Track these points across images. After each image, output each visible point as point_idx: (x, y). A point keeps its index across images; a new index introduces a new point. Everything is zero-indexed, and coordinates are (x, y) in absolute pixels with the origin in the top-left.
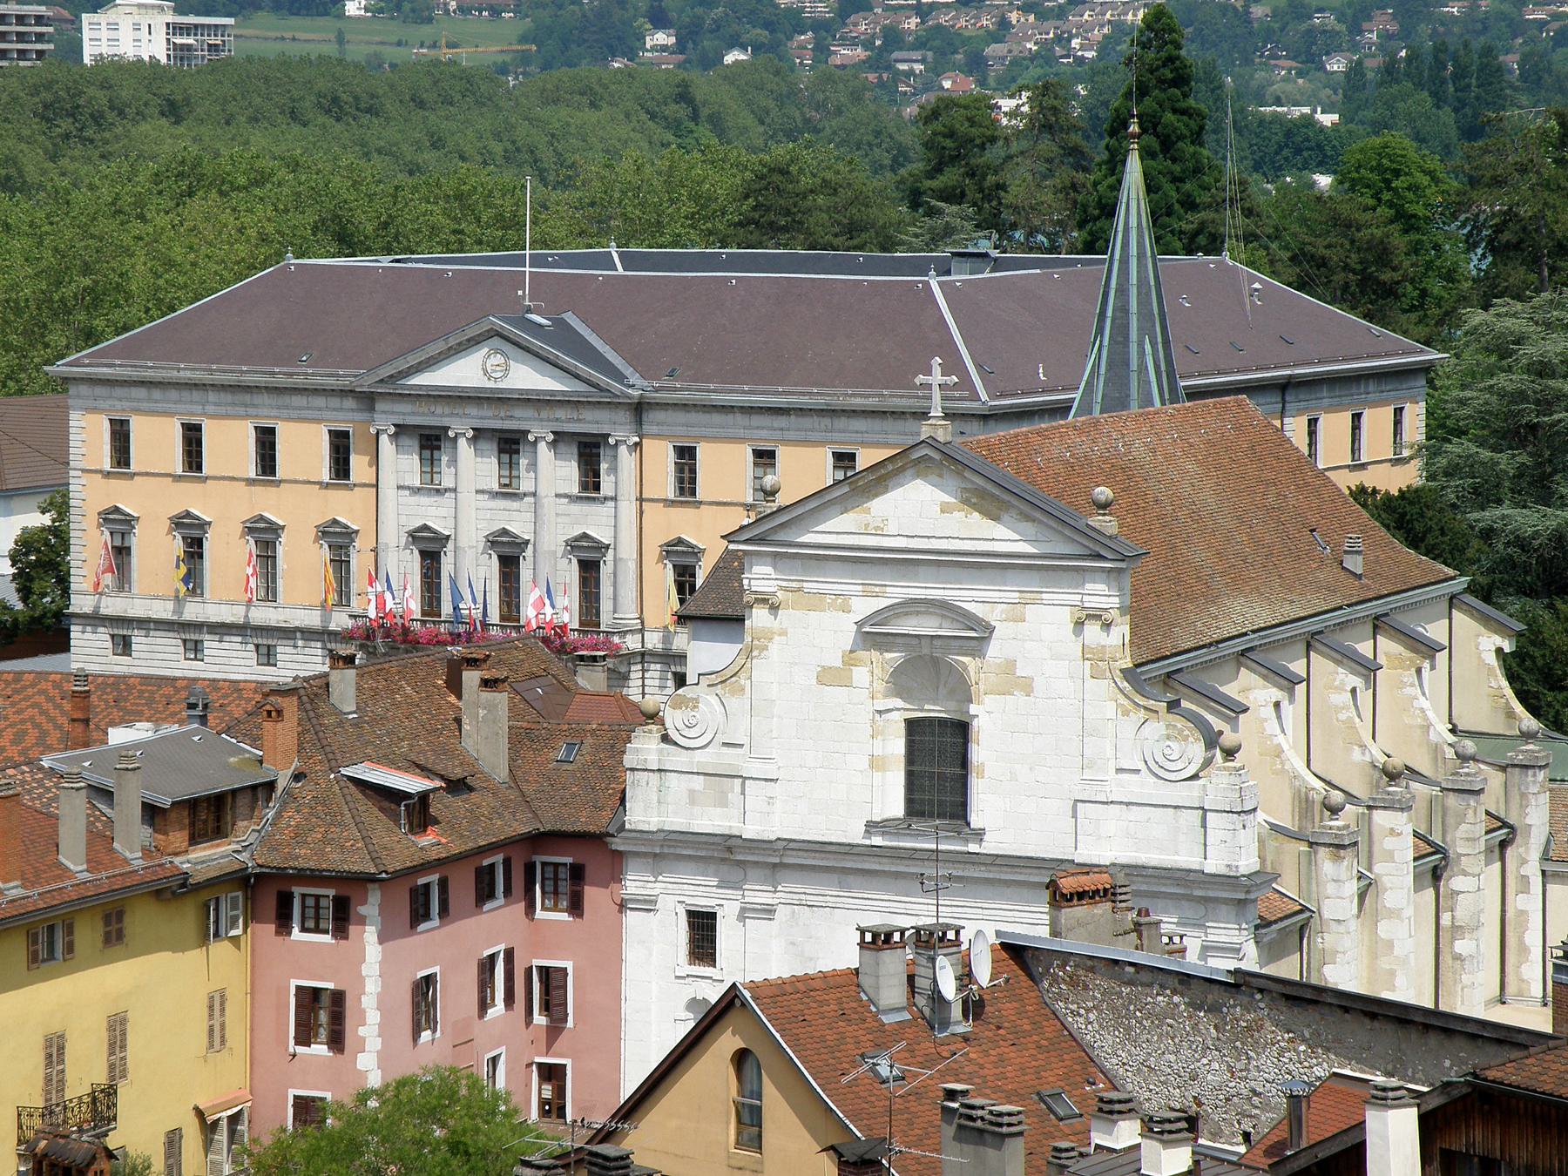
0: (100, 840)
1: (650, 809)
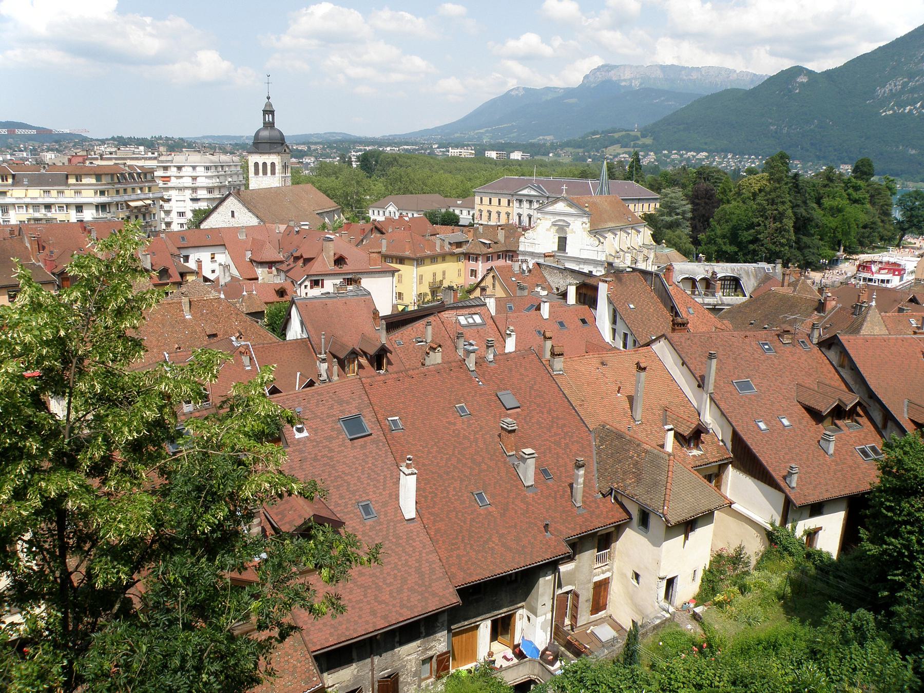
0: (442, 247)
1: (521, 248)
